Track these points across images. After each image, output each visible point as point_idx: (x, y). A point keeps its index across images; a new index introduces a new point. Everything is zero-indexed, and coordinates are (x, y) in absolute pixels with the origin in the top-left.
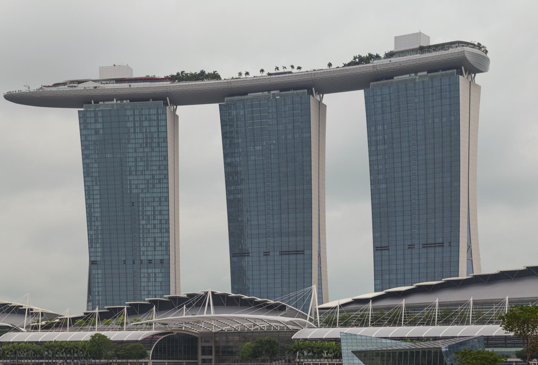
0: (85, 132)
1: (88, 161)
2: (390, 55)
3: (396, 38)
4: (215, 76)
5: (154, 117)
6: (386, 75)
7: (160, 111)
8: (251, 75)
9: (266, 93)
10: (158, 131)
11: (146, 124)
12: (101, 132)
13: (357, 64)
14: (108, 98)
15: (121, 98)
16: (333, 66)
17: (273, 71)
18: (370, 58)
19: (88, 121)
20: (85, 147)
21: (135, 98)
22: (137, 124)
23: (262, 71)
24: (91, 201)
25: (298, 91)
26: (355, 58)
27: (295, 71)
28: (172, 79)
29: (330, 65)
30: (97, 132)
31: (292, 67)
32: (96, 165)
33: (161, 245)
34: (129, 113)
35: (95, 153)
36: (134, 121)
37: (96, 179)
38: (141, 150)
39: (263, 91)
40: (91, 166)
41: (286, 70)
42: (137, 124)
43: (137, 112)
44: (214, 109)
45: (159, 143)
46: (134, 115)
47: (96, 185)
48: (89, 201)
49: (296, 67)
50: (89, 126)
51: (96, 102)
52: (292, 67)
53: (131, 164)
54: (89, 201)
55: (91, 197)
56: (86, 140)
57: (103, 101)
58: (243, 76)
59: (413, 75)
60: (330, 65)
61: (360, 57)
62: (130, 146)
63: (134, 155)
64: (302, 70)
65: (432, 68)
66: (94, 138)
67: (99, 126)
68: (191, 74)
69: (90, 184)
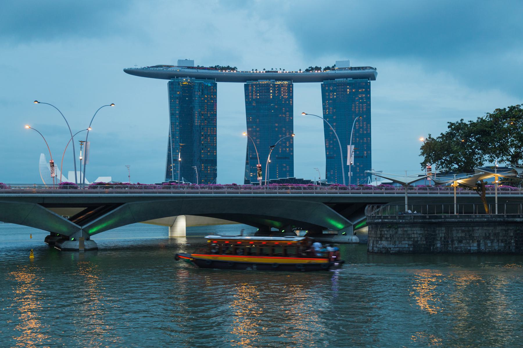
2: (333, 68)
4: (233, 69)
17: (270, 70)
18: (318, 69)
23: (264, 69)
28: (212, 68)
49: (282, 70)
61: (311, 67)
65: (355, 77)
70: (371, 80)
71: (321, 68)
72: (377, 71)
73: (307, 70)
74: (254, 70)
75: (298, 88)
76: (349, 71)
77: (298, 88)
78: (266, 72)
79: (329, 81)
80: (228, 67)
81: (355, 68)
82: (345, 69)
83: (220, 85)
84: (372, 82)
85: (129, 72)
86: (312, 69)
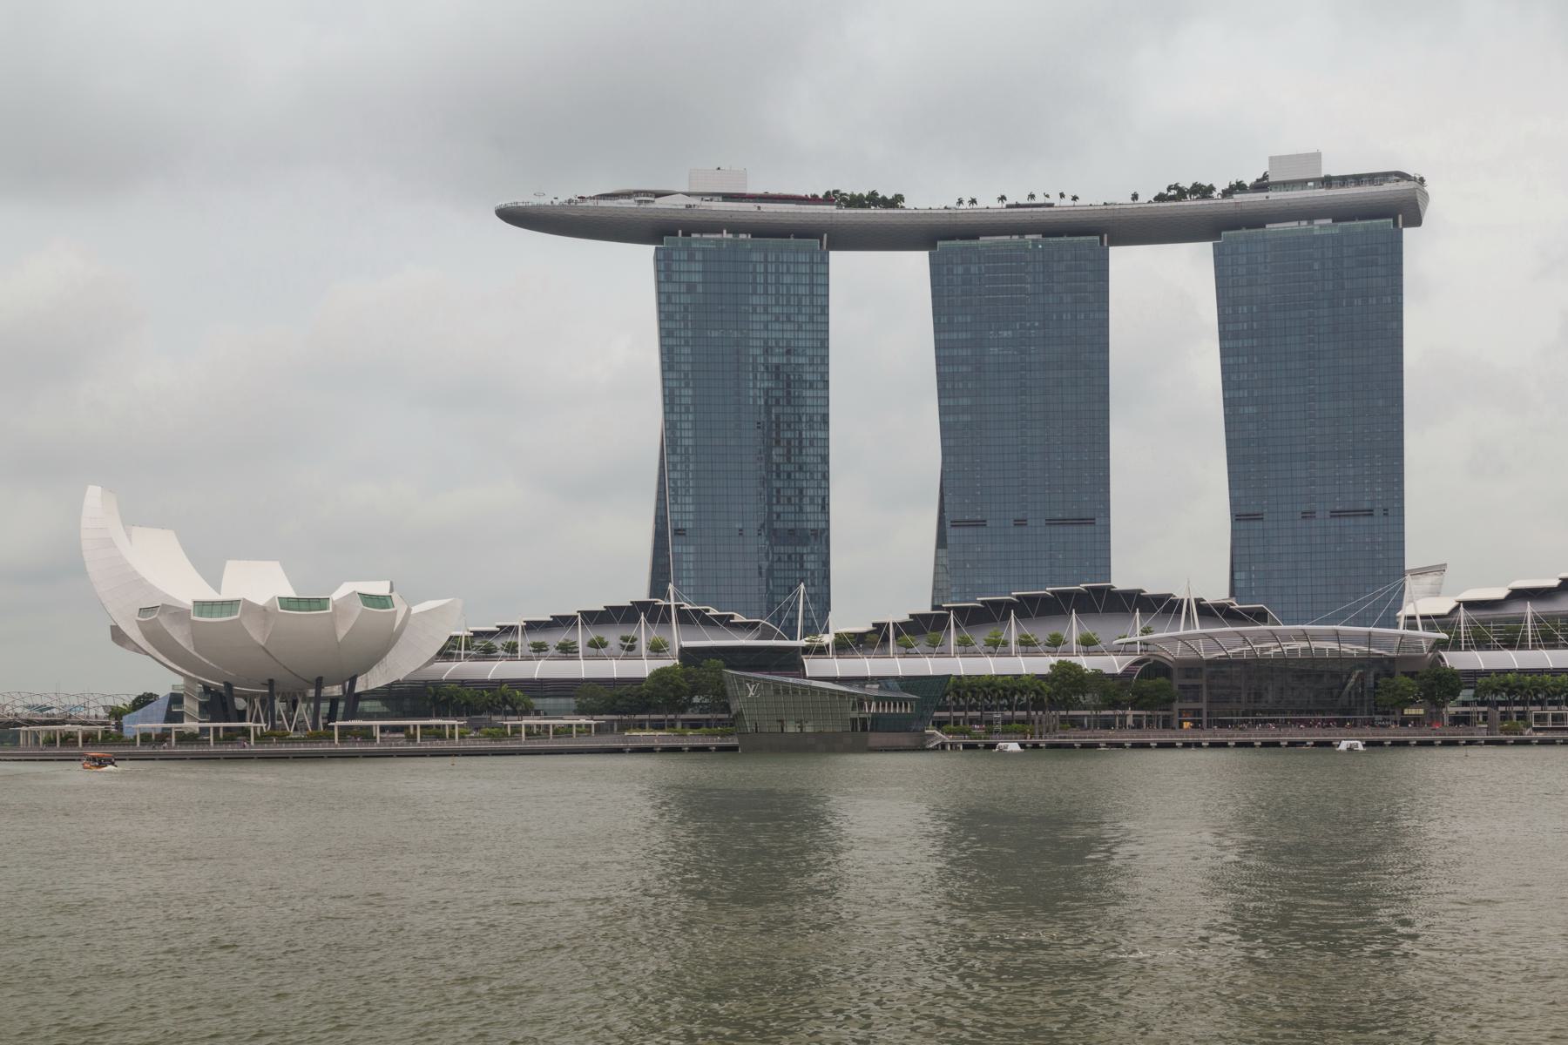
0: (668, 288)
1: (671, 342)
2: (1262, 185)
3: (1271, 159)
5: (804, 269)
6: (1255, 220)
7: (817, 258)
8: (981, 204)
9: (1016, 237)
10: (812, 294)
11: (788, 279)
12: (700, 289)
13: (1172, 198)
14: (712, 226)
15: (736, 227)
16: (1143, 199)
17: (1024, 201)
19: (675, 267)
20: (665, 316)
21: (764, 231)
22: (772, 279)
23: (1003, 198)
24: (676, 417)
25: (1076, 239)
26: (1169, 189)
27: (1067, 201)
29: (1135, 197)
30: (691, 287)
31: (1062, 195)
32: (687, 350)
33: (812, 503)
34: (756, 257)
35: (686, 328)
36: (766, 272)
37: (686, 375)
38: (777, 326)
39: (1011, 234)
40: (677, 350)
41: (1048, 201)
42: (772, 279)
43: (772, 257)
44: (916, 263)
45: (812, 315)
46: (766, 261)
47: (687, 386)
48: (671, 417)
50: (675, 277)
51: (687, 234)
52: (1062, 195)
53: (758, 352)
54: (671, 417)
55: (677, 409)
56: (669, 301)
57: (702, 232)
58: (966, 205)
59: (1304, 223)
60: (1135, 197)
61: (1176, 187)
62: (756, 318)
63: (764, 335)
64: (1078, 203)
65: (1341, 213)
66: (686, 299)
67: (697, 278)
68: (852, 196)
69: (675, 384)
70: (1408, 224)
71: (1211, 188)
72: (1429, 187)
73: (1160, 198)
74: (966, 201)
75: (1129, 267)
76: (1323, 192)
77: (1129, 267)
78: (1009, 206)
79: (1244, 231)
80: (874, 194)
81: (1344, 180)
82: (1303, 183)
83: (842, 263)
84: (1408, 234)
85: (515, 216)
86: (1181, 193)
